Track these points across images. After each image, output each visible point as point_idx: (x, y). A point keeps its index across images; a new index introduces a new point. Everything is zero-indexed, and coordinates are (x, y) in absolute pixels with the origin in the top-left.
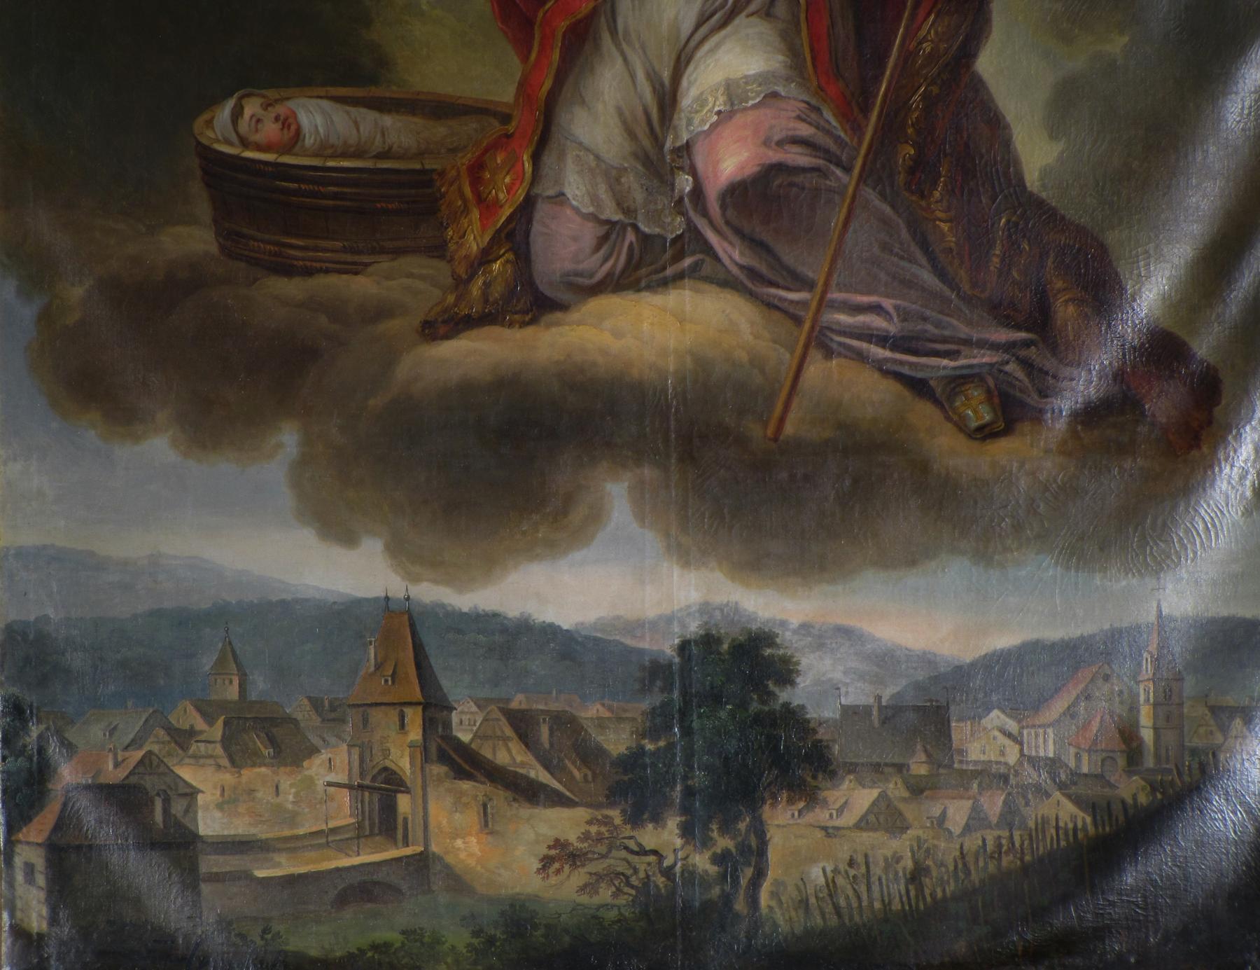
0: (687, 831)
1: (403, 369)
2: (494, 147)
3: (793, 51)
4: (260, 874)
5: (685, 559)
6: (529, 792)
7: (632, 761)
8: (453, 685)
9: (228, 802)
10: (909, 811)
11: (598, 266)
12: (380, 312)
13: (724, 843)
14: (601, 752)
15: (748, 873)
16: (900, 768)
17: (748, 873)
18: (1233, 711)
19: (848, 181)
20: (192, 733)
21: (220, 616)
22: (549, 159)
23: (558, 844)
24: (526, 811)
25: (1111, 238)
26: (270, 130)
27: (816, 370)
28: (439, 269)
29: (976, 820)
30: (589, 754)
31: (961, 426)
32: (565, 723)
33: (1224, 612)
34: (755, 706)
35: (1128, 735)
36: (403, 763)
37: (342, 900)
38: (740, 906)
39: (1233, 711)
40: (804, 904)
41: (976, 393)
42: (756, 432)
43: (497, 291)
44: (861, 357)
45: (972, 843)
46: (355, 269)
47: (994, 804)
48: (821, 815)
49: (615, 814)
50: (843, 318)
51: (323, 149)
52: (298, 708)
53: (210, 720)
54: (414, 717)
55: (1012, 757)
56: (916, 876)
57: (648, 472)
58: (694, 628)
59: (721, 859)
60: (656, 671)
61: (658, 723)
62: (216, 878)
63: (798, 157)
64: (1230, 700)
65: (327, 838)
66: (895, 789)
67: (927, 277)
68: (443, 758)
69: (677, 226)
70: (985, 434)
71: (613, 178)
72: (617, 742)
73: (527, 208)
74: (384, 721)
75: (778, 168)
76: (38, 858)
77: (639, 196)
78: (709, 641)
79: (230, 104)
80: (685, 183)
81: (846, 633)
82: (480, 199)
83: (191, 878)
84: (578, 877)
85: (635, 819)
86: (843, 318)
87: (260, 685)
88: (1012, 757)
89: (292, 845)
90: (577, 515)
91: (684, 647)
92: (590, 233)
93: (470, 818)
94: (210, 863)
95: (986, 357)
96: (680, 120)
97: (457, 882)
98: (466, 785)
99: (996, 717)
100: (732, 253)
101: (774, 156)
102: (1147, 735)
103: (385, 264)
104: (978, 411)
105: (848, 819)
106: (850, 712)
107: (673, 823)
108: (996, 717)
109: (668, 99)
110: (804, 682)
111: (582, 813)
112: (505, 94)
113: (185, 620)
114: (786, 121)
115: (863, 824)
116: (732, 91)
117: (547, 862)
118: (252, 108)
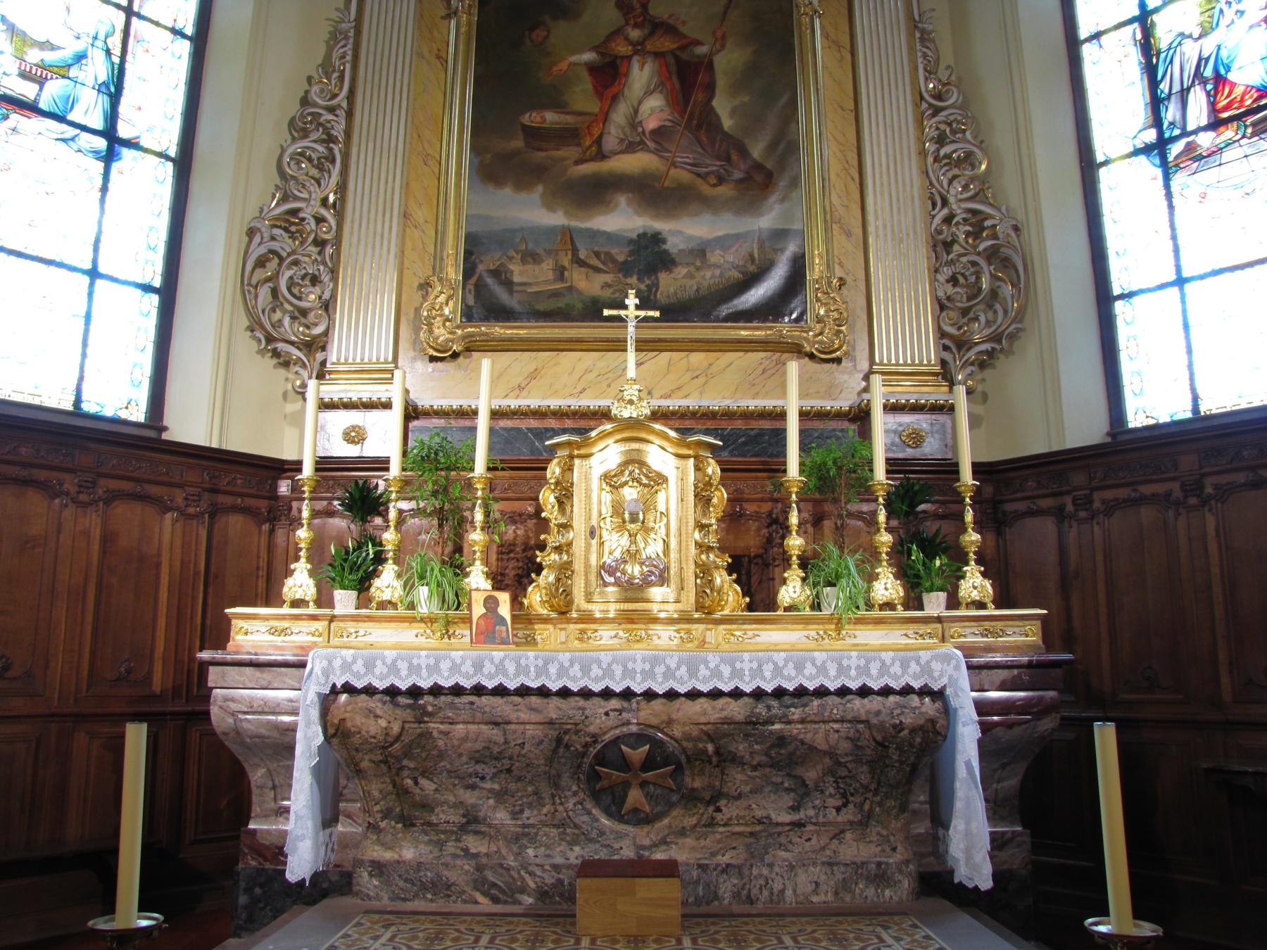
0: (639, 279)
1: (569, 172)
2: (593, 122)
3: (667, 100)
4: (529, 290)
5: (639, 215)
6: (598, 270)
7: (625, 262)
8: (579, 245)
9: (521, 274)
10: (696, 274)
11: (618, 148)
12: (564, 159)
13: (648, 282)
14: (617, 261)
15: (654, 290)
16: (693, 264)
17: (654, 290)
18: (778, 250)
19: (681, 129)
20: (513, 257)
21: (521, 229)
22: (607, 124)
23: (606, 283)
24: (597, 275)
25: (747, 141)
26: (538, 119)
27: (673, 171)
28: (580, 150)
29: (713, 276)
30: (614, 261)
31: (709, 184)
32: (607, 254)
33: (775, 227)
34: (657, 249)
35: (751, 256)
36: (566, 264)
37: (549, 297)
38: (652, 297)
39: (778, 250)
40: (668, 297)
41: (713, 176)
42: (657, 185)
43: (593, 154)
44: (684, 168)
45: (712, 282)
46: (558, 150)
47: (717, 272)
48: (672, 275)
49: (620, 275)
50: (679, 159)
51: (552, 123)
52: (540, 251)
53: (517, 254)
54: (570, 253)
55: (722, 261)
56: (697, 290)
57: (630, 195)
58: (641, 231)
59: (647, 286)
60: (631, 241)
61: (631, 253)
62: (516, 292)
63: (668, 124)
64: (777, 247)
65: (546, 282)
66: (692, 269)
67: (700, 150)
68: (577, 262)
69: (638, 139)
70: (715, 186)
71: (622, 128)
72: (621, 258)
73: (601, 136)
74: (562, 254)
75: (663, 126)
76: (472, 287)
77: (629, 133)
78: (645, 234)
79: (528, 114)
80: (640, 130)
81: (680, 232)
82: (589, 133)
83: (511, 292)
84: (611, 290)
85: (625, 276)
86: (679, 159)
87: (531, 246)
88: (722, 261)
89: (537, 284)
90: (612, 205)
91: (638, 236)
92: (617, 141)
93: (584, 277)
94: (516, 288)
95: (715, 168)
96: (639, 115)
97: (579, 292)
98: (582, 269)
99: (718, 252)
100: (651, 145)
101: (663, 123)
102: (756, 256)
103: (566, 149)
104: (713, 180)
105: (680, 276)
106: (680, 251)
107: (635, 277)
108: (718, 252)
109: (636, 111)
110: (669, 243)
111: (612, 275)
112: (596, 110)
113: (513, 231)
114: (666, 115)
115: (684, 277)
116: (652, 110)
117: (602, 287)
118: (534, 114)
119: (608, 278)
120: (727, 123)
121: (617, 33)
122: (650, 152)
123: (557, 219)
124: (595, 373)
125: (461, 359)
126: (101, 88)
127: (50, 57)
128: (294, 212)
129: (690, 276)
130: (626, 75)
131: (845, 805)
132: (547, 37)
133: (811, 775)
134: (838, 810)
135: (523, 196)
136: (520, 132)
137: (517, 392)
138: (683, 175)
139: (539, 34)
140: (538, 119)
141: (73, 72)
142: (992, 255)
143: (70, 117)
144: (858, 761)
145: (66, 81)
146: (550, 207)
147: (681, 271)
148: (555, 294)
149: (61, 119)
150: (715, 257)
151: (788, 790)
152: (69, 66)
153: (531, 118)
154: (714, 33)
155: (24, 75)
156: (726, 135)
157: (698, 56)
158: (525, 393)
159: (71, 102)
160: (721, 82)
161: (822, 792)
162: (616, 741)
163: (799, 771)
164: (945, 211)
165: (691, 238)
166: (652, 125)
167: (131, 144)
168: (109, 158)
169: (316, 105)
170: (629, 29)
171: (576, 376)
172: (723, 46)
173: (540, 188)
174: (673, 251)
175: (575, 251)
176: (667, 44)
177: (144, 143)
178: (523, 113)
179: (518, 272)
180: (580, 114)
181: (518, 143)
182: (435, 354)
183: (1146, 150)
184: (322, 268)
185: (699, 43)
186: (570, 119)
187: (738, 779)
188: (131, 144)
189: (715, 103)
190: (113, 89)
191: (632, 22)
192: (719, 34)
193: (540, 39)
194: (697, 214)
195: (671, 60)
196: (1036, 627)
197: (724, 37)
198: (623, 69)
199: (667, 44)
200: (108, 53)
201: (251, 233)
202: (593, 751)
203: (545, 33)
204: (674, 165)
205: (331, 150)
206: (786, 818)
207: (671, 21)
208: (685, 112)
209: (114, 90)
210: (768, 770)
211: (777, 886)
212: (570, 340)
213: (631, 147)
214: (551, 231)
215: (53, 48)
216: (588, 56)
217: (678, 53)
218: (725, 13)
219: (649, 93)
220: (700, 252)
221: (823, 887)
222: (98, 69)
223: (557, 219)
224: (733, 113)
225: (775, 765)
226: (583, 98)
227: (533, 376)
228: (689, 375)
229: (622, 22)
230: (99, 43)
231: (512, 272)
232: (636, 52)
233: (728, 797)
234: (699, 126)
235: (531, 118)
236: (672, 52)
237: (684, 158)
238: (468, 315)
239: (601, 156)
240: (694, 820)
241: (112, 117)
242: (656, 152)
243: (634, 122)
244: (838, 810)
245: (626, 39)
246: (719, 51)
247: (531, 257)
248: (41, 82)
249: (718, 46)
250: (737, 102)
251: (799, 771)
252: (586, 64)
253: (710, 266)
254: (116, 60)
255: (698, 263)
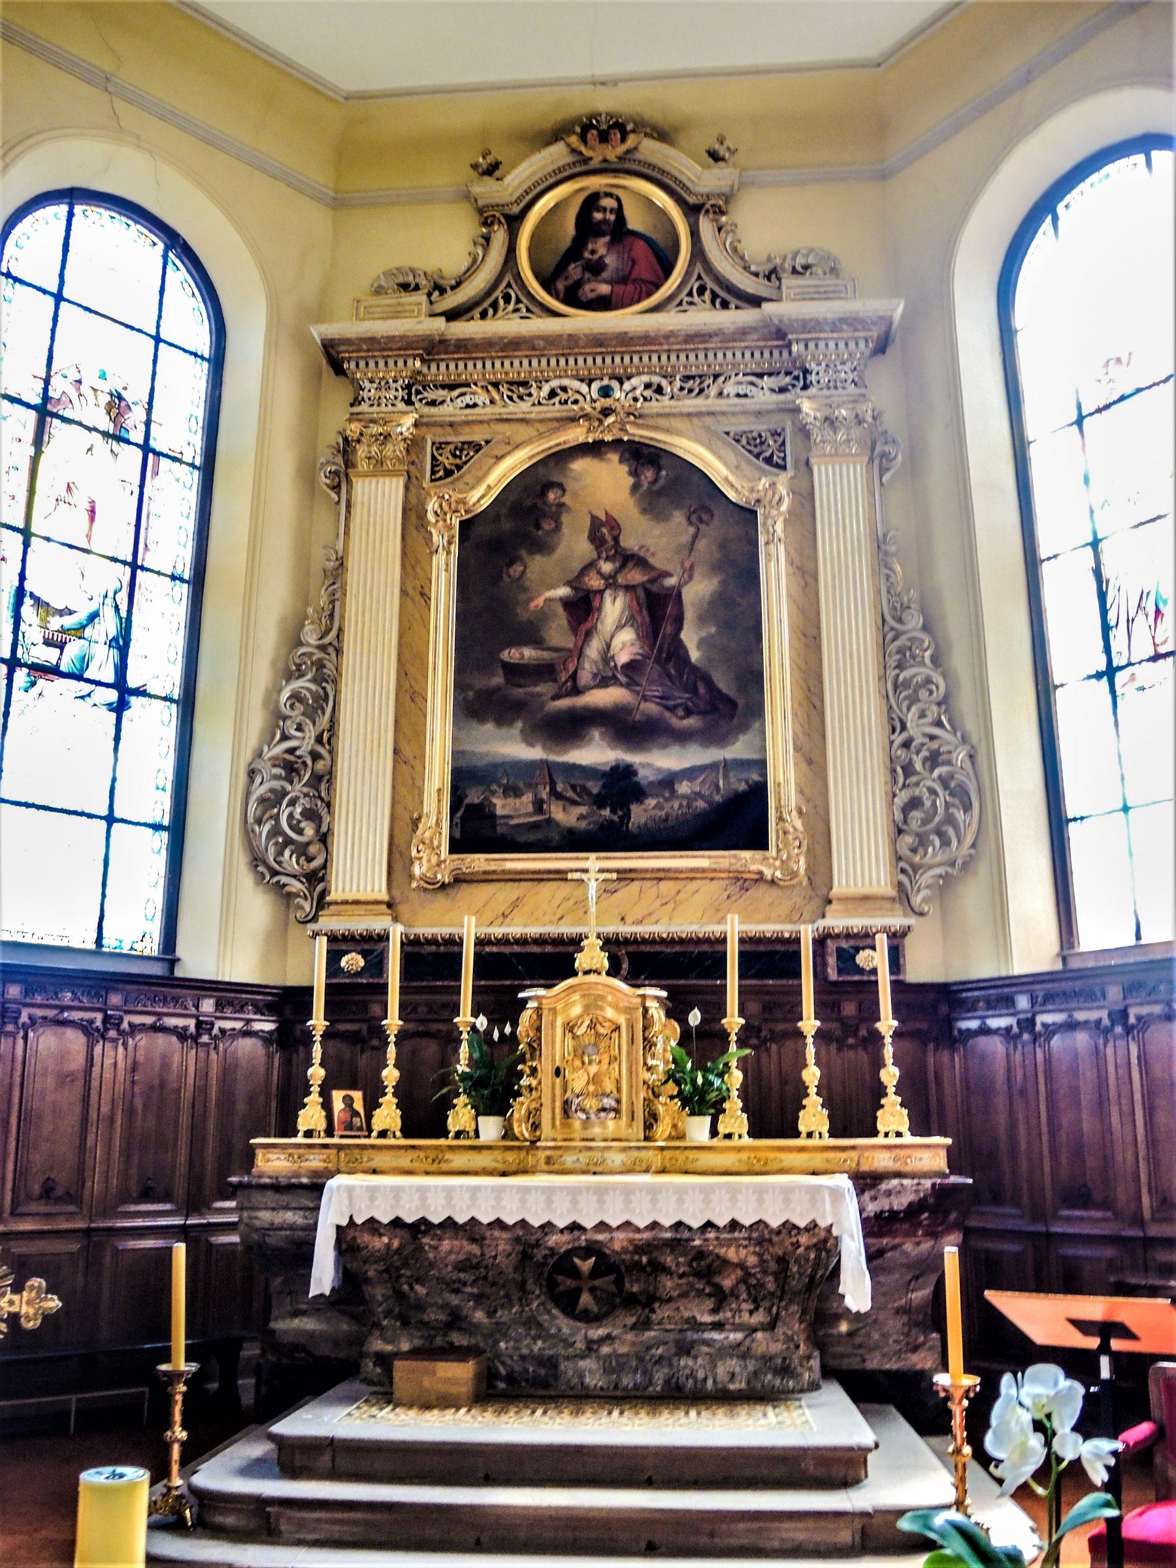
0: (611, 811)
1: (547, 708)
3: (638, 635)
5: (612, 748)
6: (574, 803)
7: (599, 794)
11: (592, 683)
13: (620, 813)
20: (496, 791)
21: (504, 764)
29: (681, 806)
30: (589, 793)
31: (677, 717)
36: (545, 796)
46: (536, 685)
48: (643, 807)
52: (521, 785)
53: (499, 787)
57: (603, 730)
60: (604, 775)
63: (639, 657)
65: (529, 815)
70: (682, 718)
72: (595, 791)
73: (575, 672)
80: (612, 664)
81: (649, 765)
89: (519, 816)
92: (590, 676)
93: (561, 809)
97: (557, 824)
104: (681, 713)
109: (609, 646)
112: (571, 645)
113: (495, 766)
119: (583, 810)
120: (695, 655)
121: (591, 565)
122: (621, 685)
123: (535, 753)
124: (572, 901)
125: (450, 891)
126: (113, 643)
127: (69, 621)
128: (291, 751)
129: (658, 806)
130: (600, 609)
131: (757, 1308)
132: (524, 572)
133: (727, 1283)
134: (751, 1313)
135: (503, 731)
136: (500, 672)
137: (501, 919)
138: (651, 708)
139: (517, 569)
140: (518, 656)
141: (88, 632)
142: (944, 781)
143: (85, 676)
144: (765, 1272)
145: (82, 641)
146: (529, 742)
147: (651, 802)
148: (534, 826)
149: (79, 677)
150: (684, 788)
151: (709, 1295)
152: (84, 627)
153: (511, 655)
154: (682, 564)
155: (48, 643)
156: (694, 669)
157: (668, 589)
158: (508, 920)
159: (85, 661)
160: (689, 615)
161: (737, 1297)
162: (569, 1253)
163: (717, 1279)
164: (904, 736)
165: (659, 770)
166: (623, 658)
167: (141, 692)
168: (120, 708)
169: (308, 645)
170: (601, 563)
171: (556, 902)
172: (691, 578)
173: (519, 725)
174: (644, 782)
175: (553, 784)
176: (636, 576)
177: (151, 690)
178: (503, 649)
179: (502, 806)
180: (556, 650)
181: (498, 680)
182: (426, 886)
183: (1098, 676)
184: (319, 803)
185: (669, 575)
186: (546, 655)
187: (668, 1285)
188: (141, 692)
189: (684, 635)
190: (121, 642)
191: (604, 555)
192: (687, 565)
193: (517, 575)
194: (665, 747)
195: (641, 592)
196: (943, 1154)
197: (692, 567)
198: (596, 604)
199: (636, 576)
200: (117, 608)
201: (252, 773)
202: (551, 1261)
203: (522, 568)
204: (645, 698)
205: (324, 688)
206: (707, 1319)
207: (642, 554)
208: (655, 644)
209: (122, 643)
210: (691, 1279)
211: (701, 1375)
212: (550, 872)
213: (604, 681)
214: (533, 765)
215: (71, 613)
216: (563, 591)
217: (648, 586)
218: (693, 543)
219: (620, 627)
220: (668, 782)
221: (738, 1378)
222: (108, 626)
223: (535, 753)
224: (701, 643)
225: (698, 1274)
226: (558, 633)
227: (516, 904)
228: (658, 903)
229: (595, 555)
230: (109, 601)
231: (495, 805)
232: (608, 586)
233: (660, 1300)
234: (668, 659)
235: (511, 655)
236: (643, 585)
237: (656, 691)
238: (456, 847)
239: (577, 691)
240: (634, 1319)
241: (121, 669)
242: (627, 686)
243: (606, 656)
244: (751, 1313)
245: (599, 572)
246: (686, 583)
247: (512, 791)
248: (61, 646)
249: (686, 576)
250: (704, 634)
251: (717, 1279)
252: (561, 599)
253: (677, 797)
254: (124, 614)
255: (667, 795)
